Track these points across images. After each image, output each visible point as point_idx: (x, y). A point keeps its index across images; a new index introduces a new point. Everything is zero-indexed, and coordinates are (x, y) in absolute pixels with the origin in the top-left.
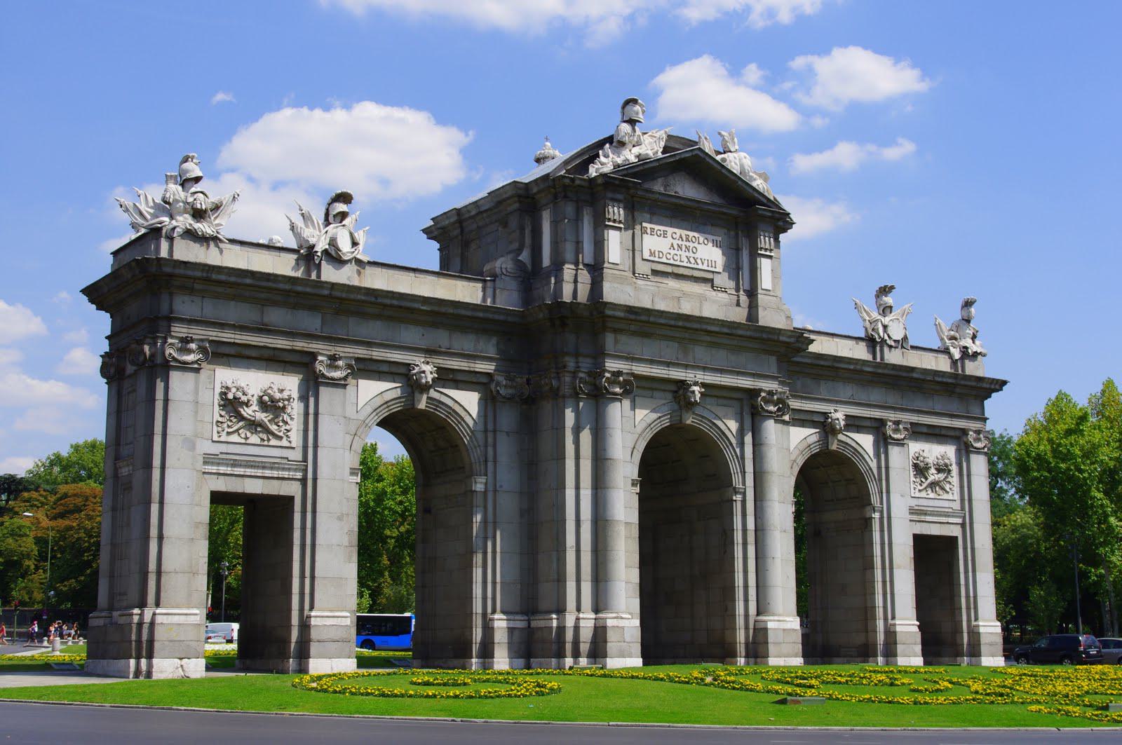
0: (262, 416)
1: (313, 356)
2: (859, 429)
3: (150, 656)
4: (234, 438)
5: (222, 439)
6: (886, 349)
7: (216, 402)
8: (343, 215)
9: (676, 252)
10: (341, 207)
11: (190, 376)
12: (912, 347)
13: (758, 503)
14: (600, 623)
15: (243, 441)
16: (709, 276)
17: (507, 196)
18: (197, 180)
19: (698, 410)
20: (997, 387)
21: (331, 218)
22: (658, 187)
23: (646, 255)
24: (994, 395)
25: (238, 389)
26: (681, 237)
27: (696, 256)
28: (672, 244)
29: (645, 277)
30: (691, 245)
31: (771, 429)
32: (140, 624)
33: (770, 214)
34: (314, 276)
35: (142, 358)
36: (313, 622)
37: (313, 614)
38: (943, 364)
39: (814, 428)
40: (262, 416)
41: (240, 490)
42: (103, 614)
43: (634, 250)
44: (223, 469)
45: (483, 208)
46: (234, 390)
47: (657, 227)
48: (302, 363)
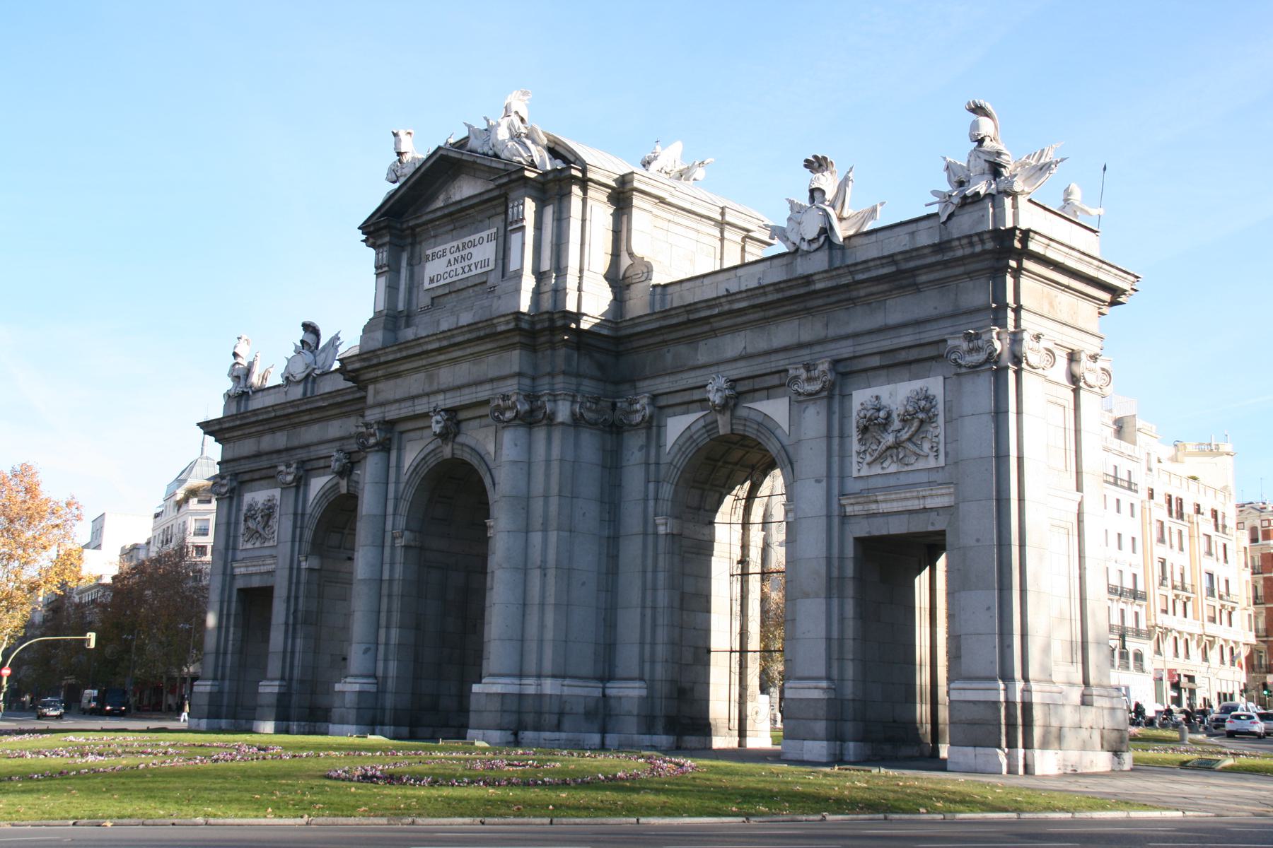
2: (769, 392)
4: (249, 546)
5: (244, 548)
6: (799, 259)
7: (243, 518)
9: (453, 268)
16: (485, 279)
19: (460, 439)
22: (439, 203)
23: (427, 285)
26: (458, 247)
27: (470, 262)
28: (450, 262)
29: (426, 310)
30: (466, 252)
36: (261, 690)
37: (261, 683)
39: (703, 411)
41: (249, 586)
44: (243, 570)
47: (436, 250)
48: (269, 477)
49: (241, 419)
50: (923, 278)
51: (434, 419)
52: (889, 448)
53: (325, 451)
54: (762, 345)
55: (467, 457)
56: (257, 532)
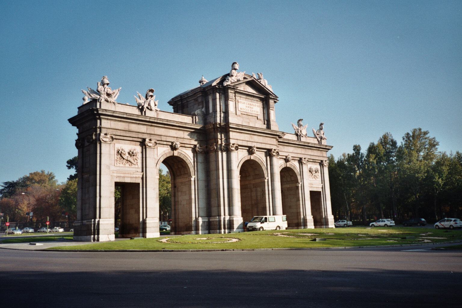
0: (130, 158)
1: (144, 140)
3: (98, 234)
5: (118, 165)
6: (301, 138)
8: (152, 96)
10: (151, 94)
11: (108, 145)
12: (308, 137)
13: (272, 182)
14: (231, 219)
15: (124, 166)
16: (257, 116)
17: (198, 91)
18: (108, 84)
20: (330, 148)
21: (148, 97)
24: (329, 150)
25: (122, 150)
26: (249, 104)
30: (251, 106)
31: (275, 159)
32: (94, 224)
33: (273, 97)
34: (143, 114)
35: (91, 140)
36: (147, 221)
38: (315, 141)
40: (130, 158)
41: (124, 181)
42: (80, 222)
43: (236, 108)
45: (189, 96)
46: (121, 150)
49: (127, 115)
50: (320, 149)
51: (255, 149)
52: (315, 176)
53: (169, 140)
54: (296, 151)
55: (257, 160)
56: (129, 161)
